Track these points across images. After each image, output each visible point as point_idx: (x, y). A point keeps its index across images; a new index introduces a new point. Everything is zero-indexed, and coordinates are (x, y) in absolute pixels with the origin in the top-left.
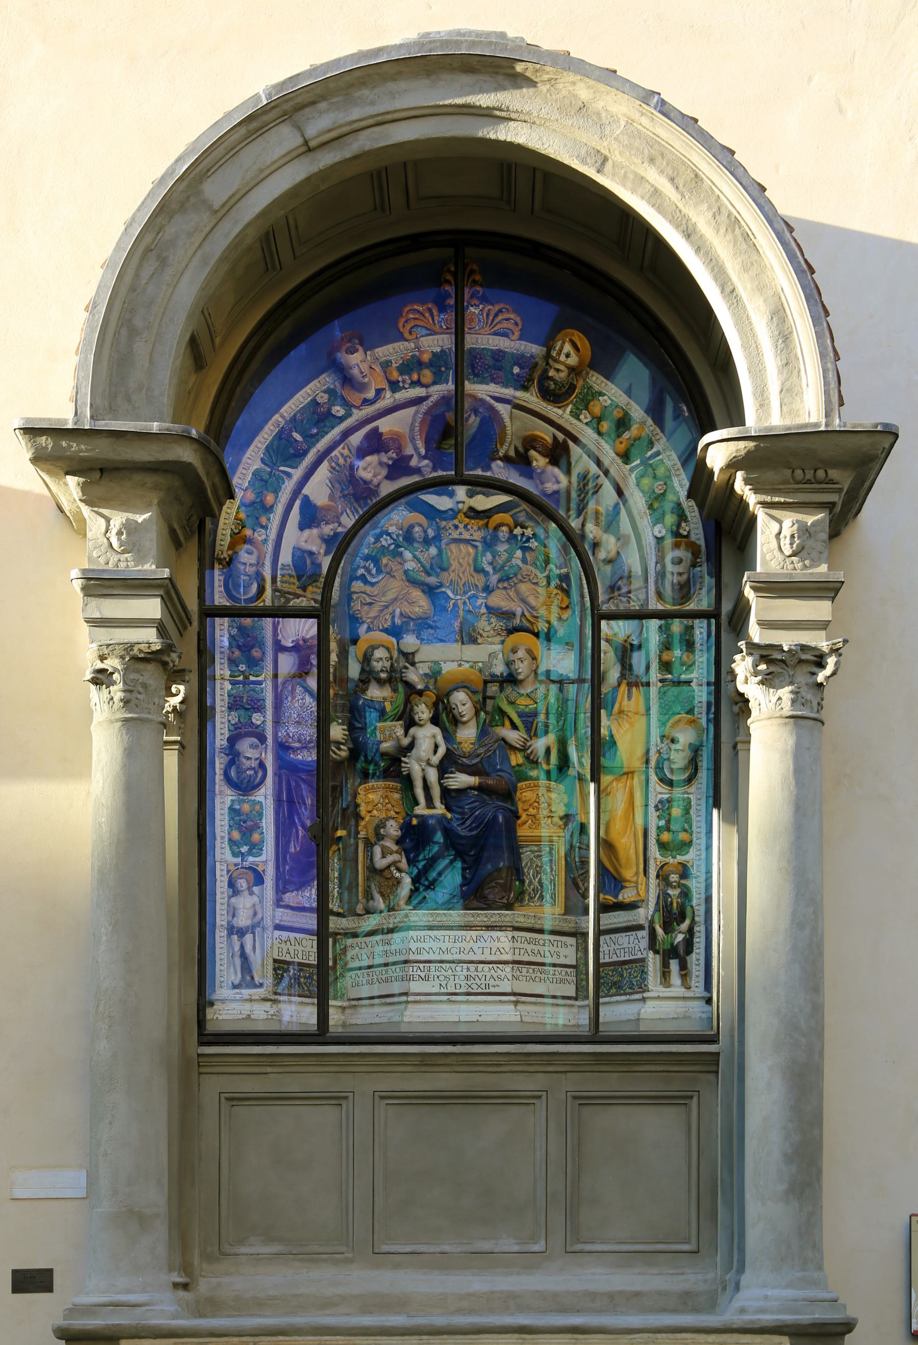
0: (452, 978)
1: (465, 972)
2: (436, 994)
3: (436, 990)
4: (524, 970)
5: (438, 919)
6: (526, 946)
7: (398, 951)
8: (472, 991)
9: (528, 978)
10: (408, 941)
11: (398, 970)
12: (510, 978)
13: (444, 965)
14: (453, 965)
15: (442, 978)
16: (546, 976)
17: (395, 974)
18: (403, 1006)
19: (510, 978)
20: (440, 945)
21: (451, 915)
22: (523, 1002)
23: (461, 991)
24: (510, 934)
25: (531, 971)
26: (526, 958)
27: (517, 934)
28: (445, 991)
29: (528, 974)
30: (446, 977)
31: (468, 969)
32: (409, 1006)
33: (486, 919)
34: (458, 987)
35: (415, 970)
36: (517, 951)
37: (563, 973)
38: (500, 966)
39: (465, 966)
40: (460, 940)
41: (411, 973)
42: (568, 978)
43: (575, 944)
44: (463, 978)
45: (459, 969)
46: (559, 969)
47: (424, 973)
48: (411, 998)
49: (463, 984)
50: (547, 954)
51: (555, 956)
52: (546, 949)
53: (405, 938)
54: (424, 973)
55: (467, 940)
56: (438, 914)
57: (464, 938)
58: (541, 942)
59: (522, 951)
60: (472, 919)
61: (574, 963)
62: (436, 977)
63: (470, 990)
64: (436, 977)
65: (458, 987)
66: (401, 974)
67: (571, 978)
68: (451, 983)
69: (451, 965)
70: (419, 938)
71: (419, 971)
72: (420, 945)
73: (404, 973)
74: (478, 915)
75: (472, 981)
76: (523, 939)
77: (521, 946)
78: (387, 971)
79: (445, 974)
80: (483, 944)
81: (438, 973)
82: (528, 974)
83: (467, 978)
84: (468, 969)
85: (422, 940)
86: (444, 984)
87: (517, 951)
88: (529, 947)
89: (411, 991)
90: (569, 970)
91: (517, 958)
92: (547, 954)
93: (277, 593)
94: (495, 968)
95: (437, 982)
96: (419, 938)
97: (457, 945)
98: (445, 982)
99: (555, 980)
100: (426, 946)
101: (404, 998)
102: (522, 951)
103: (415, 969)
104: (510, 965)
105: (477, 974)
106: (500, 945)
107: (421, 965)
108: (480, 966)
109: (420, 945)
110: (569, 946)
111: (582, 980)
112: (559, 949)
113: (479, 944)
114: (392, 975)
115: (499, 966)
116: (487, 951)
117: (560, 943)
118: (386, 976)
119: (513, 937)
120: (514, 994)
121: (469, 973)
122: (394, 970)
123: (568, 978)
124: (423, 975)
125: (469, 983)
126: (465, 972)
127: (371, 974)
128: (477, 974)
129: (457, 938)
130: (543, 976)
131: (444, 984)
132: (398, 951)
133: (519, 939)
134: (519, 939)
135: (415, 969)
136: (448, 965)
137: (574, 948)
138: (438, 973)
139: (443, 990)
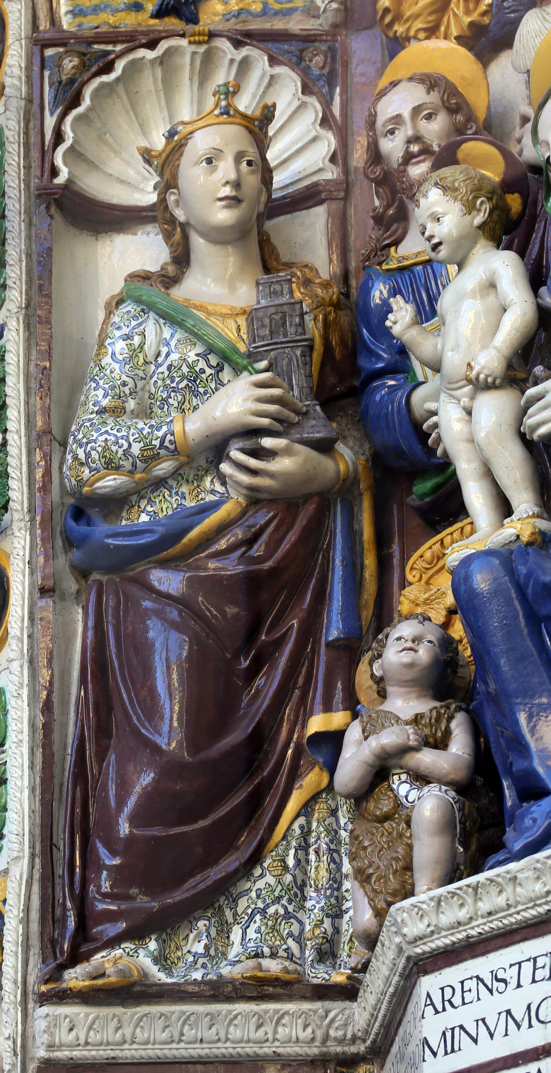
56: (476, 888)
93: (49, 52)
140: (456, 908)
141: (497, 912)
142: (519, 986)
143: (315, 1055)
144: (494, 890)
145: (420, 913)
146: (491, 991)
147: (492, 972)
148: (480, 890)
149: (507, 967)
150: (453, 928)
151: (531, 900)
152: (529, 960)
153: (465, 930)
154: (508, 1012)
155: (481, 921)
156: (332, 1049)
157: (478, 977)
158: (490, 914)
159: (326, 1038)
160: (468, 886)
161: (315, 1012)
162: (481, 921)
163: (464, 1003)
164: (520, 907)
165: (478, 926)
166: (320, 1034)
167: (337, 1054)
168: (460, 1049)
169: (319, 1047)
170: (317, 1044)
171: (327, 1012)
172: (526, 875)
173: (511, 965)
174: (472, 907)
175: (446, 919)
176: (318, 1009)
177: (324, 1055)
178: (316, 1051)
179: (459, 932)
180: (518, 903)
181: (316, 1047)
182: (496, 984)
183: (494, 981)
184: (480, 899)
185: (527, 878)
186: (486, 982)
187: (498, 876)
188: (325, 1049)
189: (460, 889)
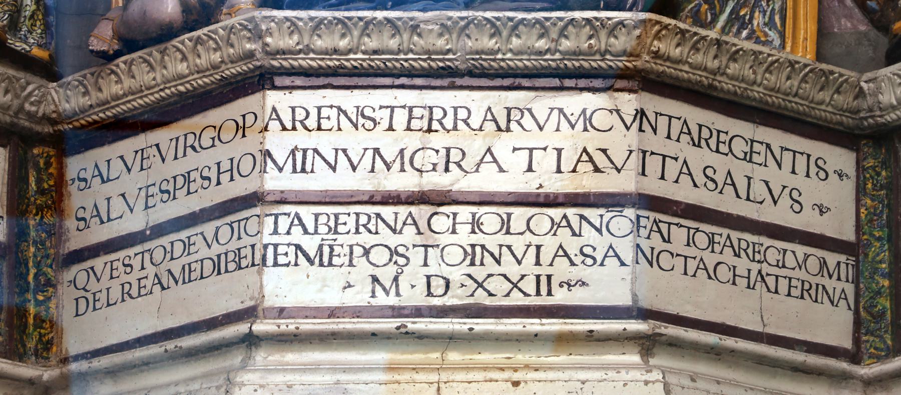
0: (417, 255)
1: (464, 236)
2: (357, 312)
3: (359, 297)
4: (679, 235)
5: (371, 43)
6: (684, 149)
7: (226, 166)
8: (489, 302)
9: (692, 265)
10: (260, 124)
11: (225, 232)
12: (628, 255)
13: (387, 212)
14: (421, 212)
15: (380, 256)
16: (755, 267)
17: (216, 249)
18: (236, 358)
19: (628, 257)
20: (380, 139)
21: (415, 29)
22: (675, 345)
23: (450, 301)
24: (629, 102)
25: (701, 240)
26: (684, 193)
27: (653, 103)
28: (392, 300)
29: (691, 251)
30: (394, 252)
31: (476, 225)
32: (261, 356)
33: (542, 44)
34: (438, 286)
35: (283, 228)
36: (654, 163)
37: (813, 264)
38: (592, 214)
39: (465, 212)
40: (449, 123)
41: (267, 239)
42: (830, 284)
43: (851, 170)
44: (455, 255)
45: (441, 223)
46: (801, 250)
47: (317, 239)
48: (261, 327)
49: (456, 275)
50: (759, 190)
51: (785, 201)
52: (759, 173)
53: (250, 119)
54: (317, 239)
55: (475, 122)
56: (368, 23)
57: (462, 114)
58: (739, 147)
59: (672, 169)
60: (491, 44)
61: (849, 235)
62: (358, 251)
63: (481, 297)
64: (358, 251)
65: (438, 286)
66: (234, 245)
67: (839, 286)
68: (414, 274)
69: (413, 209)
70: (300, 114)
71: (297, 230)
72: (301, 139)
73: (247, 241)
74: (515, 28)
75: (491, 266)
76: (676, 126)
77: (670, 148)
78: (187, 245)
79: (393, 240)
80: (535, 139)
81: (366, 239)
82: (691, 251)
83: (471, 255)
84: (476, 225)
85: (312, 123)
86: (386, 275)
87: (654, 163)
88: (699, 158)
89: (270, 302)
90: (832, 259)
91: (654, 187)
92: (759, 190)
94: (575, 221)
95: (363, 268)
96: (300, 114)
97: (439, 140)
98: (392, 270)
99: (783, 285)
100: (326, 143)
101: (242, 328)
102: (672, 169)
103: (284, 223)
104: (630, 212)
105: (508, 240)
106: (593, 140)
107: (307, 213)
108: (520, 214)
109: (301, 139)
110: (833, 177)
111: (879, 293)
112: (799, 181)
113: (517, 137)
114: (204, 252)
115: (587, 212)
116: (545, 162)
117: (801, 161)
118: (185, 260)
119: (641, 114)
120: (645, 314)
121: (478, 238)
122: (210, 238)
123: (830, 284)
124: (310, 244)
125: (479, 273)
126: (464, 236)
127: (136, 263)
128: (508, 240)
129: (438, 113)
130: (743, 264)
131: (386, 275)
132: (226, 166)
133: (663, 122)
134: (663, 122)
135: (284, 223)
136: (403, 211)
137: (848, 187)
138: (366, 239)
139: (382, 299)
140: (337, 36)
141: (383, 53)
142: (391, 128)
143: (6, 123)
144: (387, 31)
145: (292, 29)
146: (356, 126)
147: (358, 107)
148: (371, 26)
149: (377, 108)
150: (327, 54)
151: (428, 52)
152: (404, 107)
153: (339, 60)
154: (377, 151)
155: (360, 56)
156: (22, 122)
157: (339, 109)
158: (375, 52)
159: (21, 109)
160: (360, 19)
161: (18, 80)
162: (360, 56)
163: (319, 128)
164: (411, 56)
165: (355, 60)
166: (16, 103)
167: (24, 128)
168: (312, 171)
169: (11, 116)
170: (11, 113)
171: (28, 84)
172: (430, 27)
173: (381, 107)
174: (355, 40)
175: (319, 43)
176: (21, 79)
177: (13, 124)
178: (8, 119)
179: (331, 60)
180: (412, 51)
181: (9, 115)
182: (361, 121)
183: (360, 117)
184: (369, 36)
185: (431, 31)
186: (349, 115)
187: (399, 19)
188: (15, 120)
189: (350, 19)
